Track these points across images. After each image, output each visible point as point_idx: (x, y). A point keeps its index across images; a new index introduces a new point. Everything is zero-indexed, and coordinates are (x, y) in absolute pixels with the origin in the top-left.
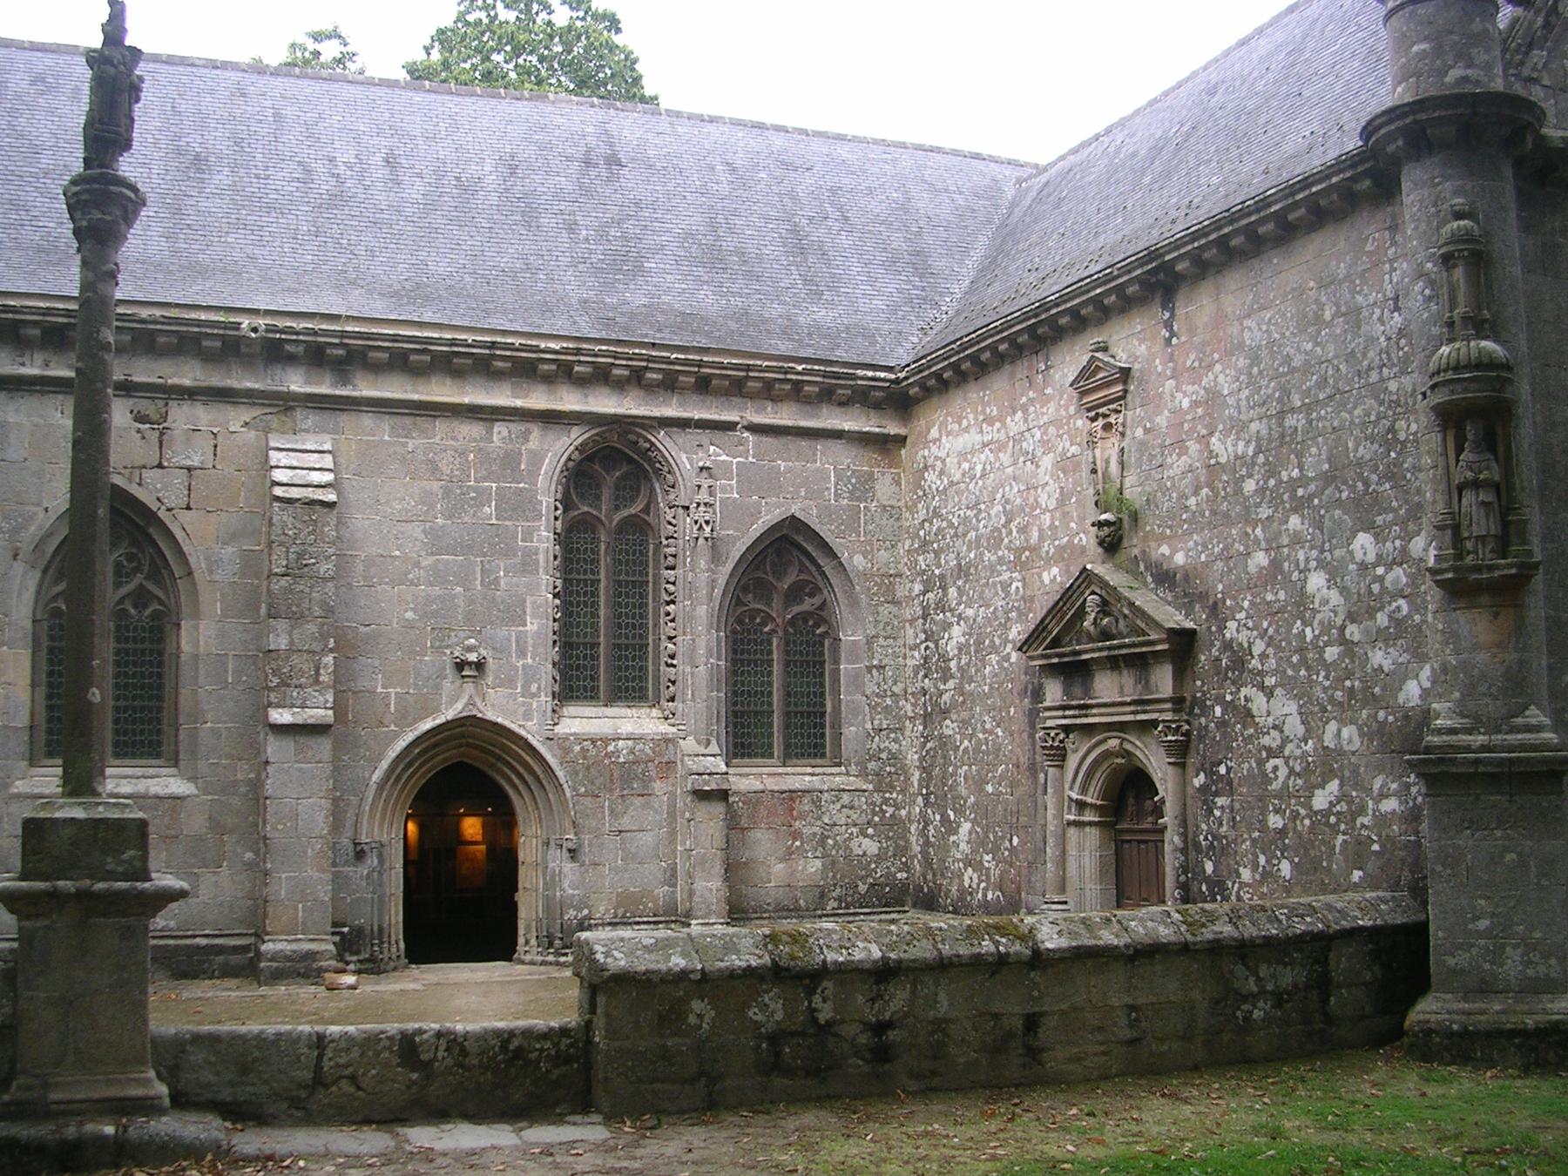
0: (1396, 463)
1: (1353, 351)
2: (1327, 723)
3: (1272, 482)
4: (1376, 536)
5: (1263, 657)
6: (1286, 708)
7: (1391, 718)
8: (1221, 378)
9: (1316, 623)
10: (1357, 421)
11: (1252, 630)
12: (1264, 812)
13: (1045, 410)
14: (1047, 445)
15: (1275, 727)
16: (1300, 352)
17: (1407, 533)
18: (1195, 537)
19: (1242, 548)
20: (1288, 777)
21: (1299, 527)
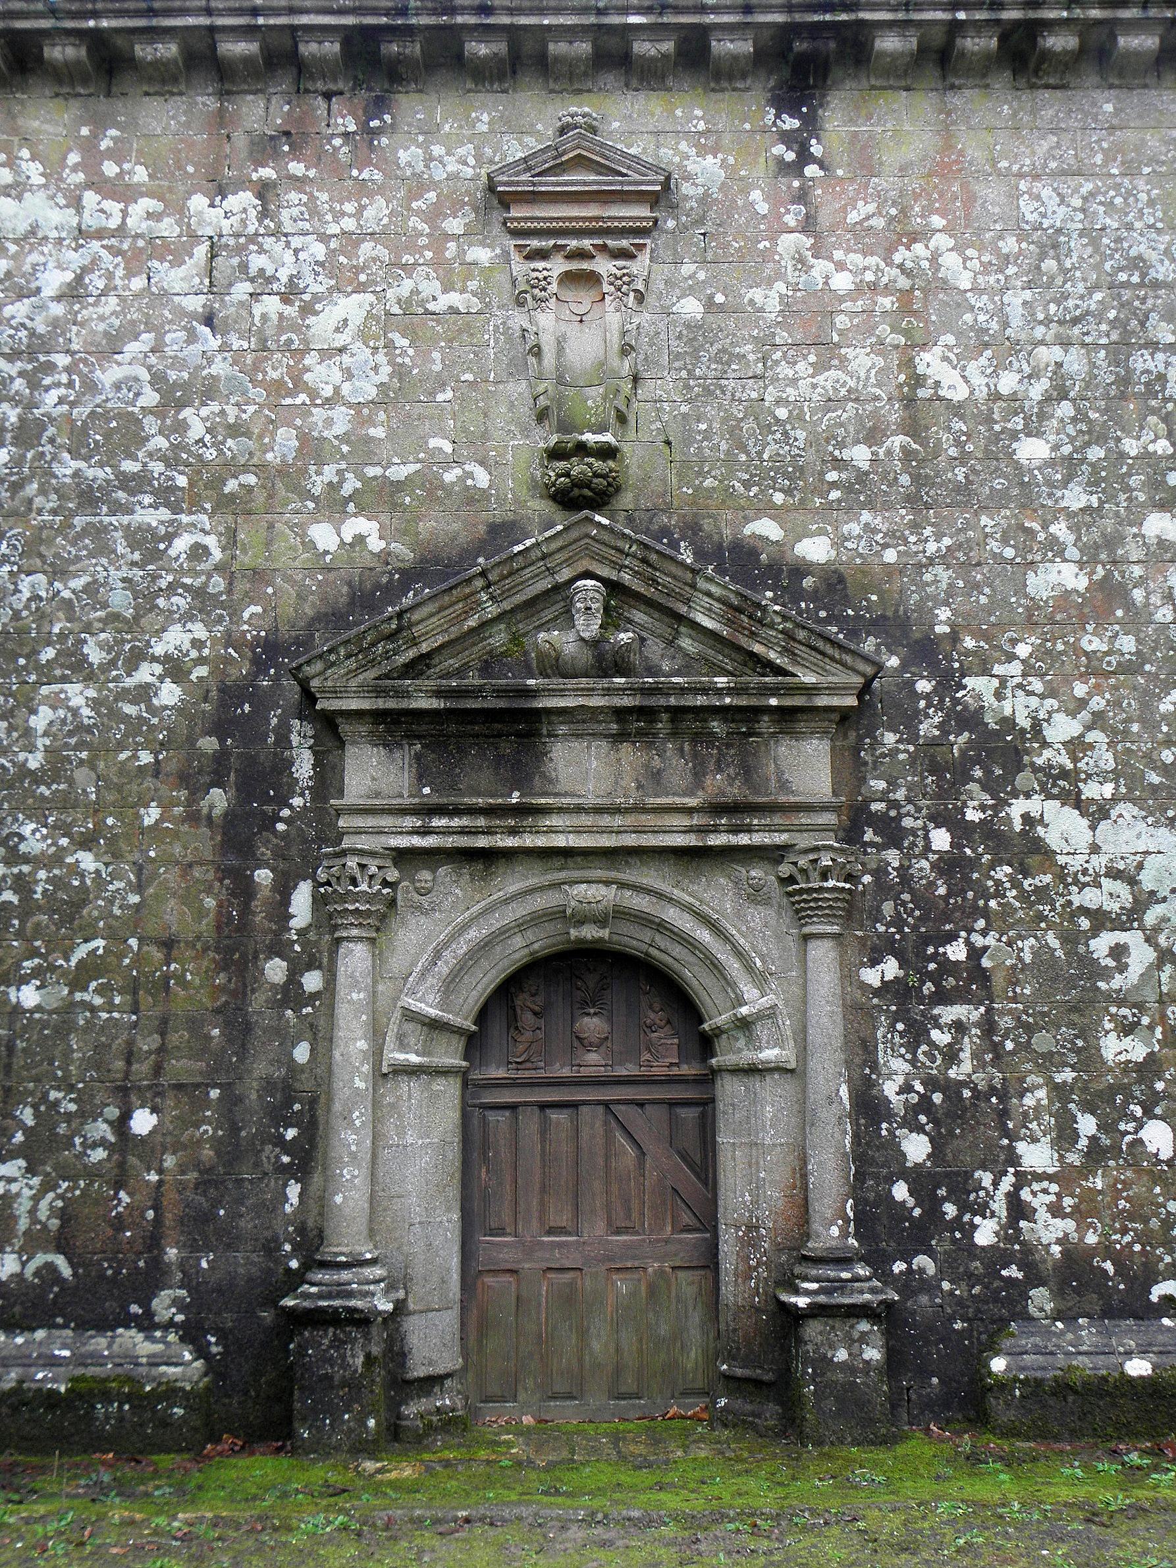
3: (1096, 453)
5: (1076, 747)
8: (950, 261)
11: (1042, 697)
12: (1090, 1033)
13: (349, 207)
15: (1114, 874)
18: (866, 516)
20: (1159, 965)
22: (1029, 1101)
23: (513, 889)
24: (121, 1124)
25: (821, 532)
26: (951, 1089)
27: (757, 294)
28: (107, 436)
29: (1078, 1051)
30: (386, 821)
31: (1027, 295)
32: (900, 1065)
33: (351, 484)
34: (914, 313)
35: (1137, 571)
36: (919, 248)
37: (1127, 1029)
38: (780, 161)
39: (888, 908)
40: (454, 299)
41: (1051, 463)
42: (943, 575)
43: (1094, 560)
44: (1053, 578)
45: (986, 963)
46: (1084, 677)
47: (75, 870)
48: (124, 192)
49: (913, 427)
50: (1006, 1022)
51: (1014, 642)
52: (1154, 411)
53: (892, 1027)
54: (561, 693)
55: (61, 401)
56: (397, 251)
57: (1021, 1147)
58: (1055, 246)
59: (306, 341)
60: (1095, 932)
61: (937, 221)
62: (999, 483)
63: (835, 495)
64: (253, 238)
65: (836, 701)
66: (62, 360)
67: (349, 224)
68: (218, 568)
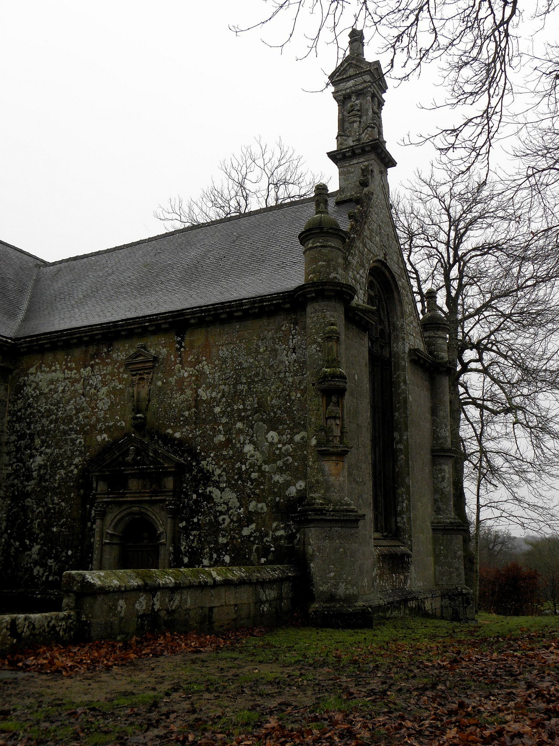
0: (289, 407)
1: (273, 365)
2: (250, 502)
3: (229, 409)
4: (278, 433)
5: (220, 476)
6: (231, 496)
7: (282, 500)
8: (206, 367)
9: (247, 464)
10: (273, 390)
12: (217, 537)
13: (105, 368)
14: (104, 384)
15: (224, 503)
16: (247, 362)
17: (294, 433)
18: (187, 427)
19: (211, 433)
20: (230, 523)
21: (241, 427)
22: (205, 551)
23: (124, 508)
24: (67, 553)
25: (179, 431)
26: (192, 548)
27: (171, 379)
28: (68, 420)
29: (214, 540)
30: (103, 496)
31: (219, 374)
32: (184, 543)
33: (104, 427)
34: (198, 380)
35: (234, 436)
36: (200, 365)
37: (224, 536)
38: (177, 347)
39: (185, 511)
40: (121, 386)
41: (220, 412)
42: (199, 439)
43: (226, 434)
44: (219, 439)
45: (200, 522)
46: (222, 460)
47: (62, 506)
48: (70, 369)
49: (196, 407)
50: (203, 535)
51: (211, 453)
52: (240, 398)
53: (183, 536)
54: (127, 470)
55: (61, 414)
56: (112, 377)
57: (203, 560)
58: (225, 362)
59: (98, 398)
60: (220, 516)
61: (204, 358)
62: (211, 418)
63: (182, 423)
64: (90, 377)
65: (171, 470)
66: (61, 405)
67: (105, 372)
68: (83, 446)
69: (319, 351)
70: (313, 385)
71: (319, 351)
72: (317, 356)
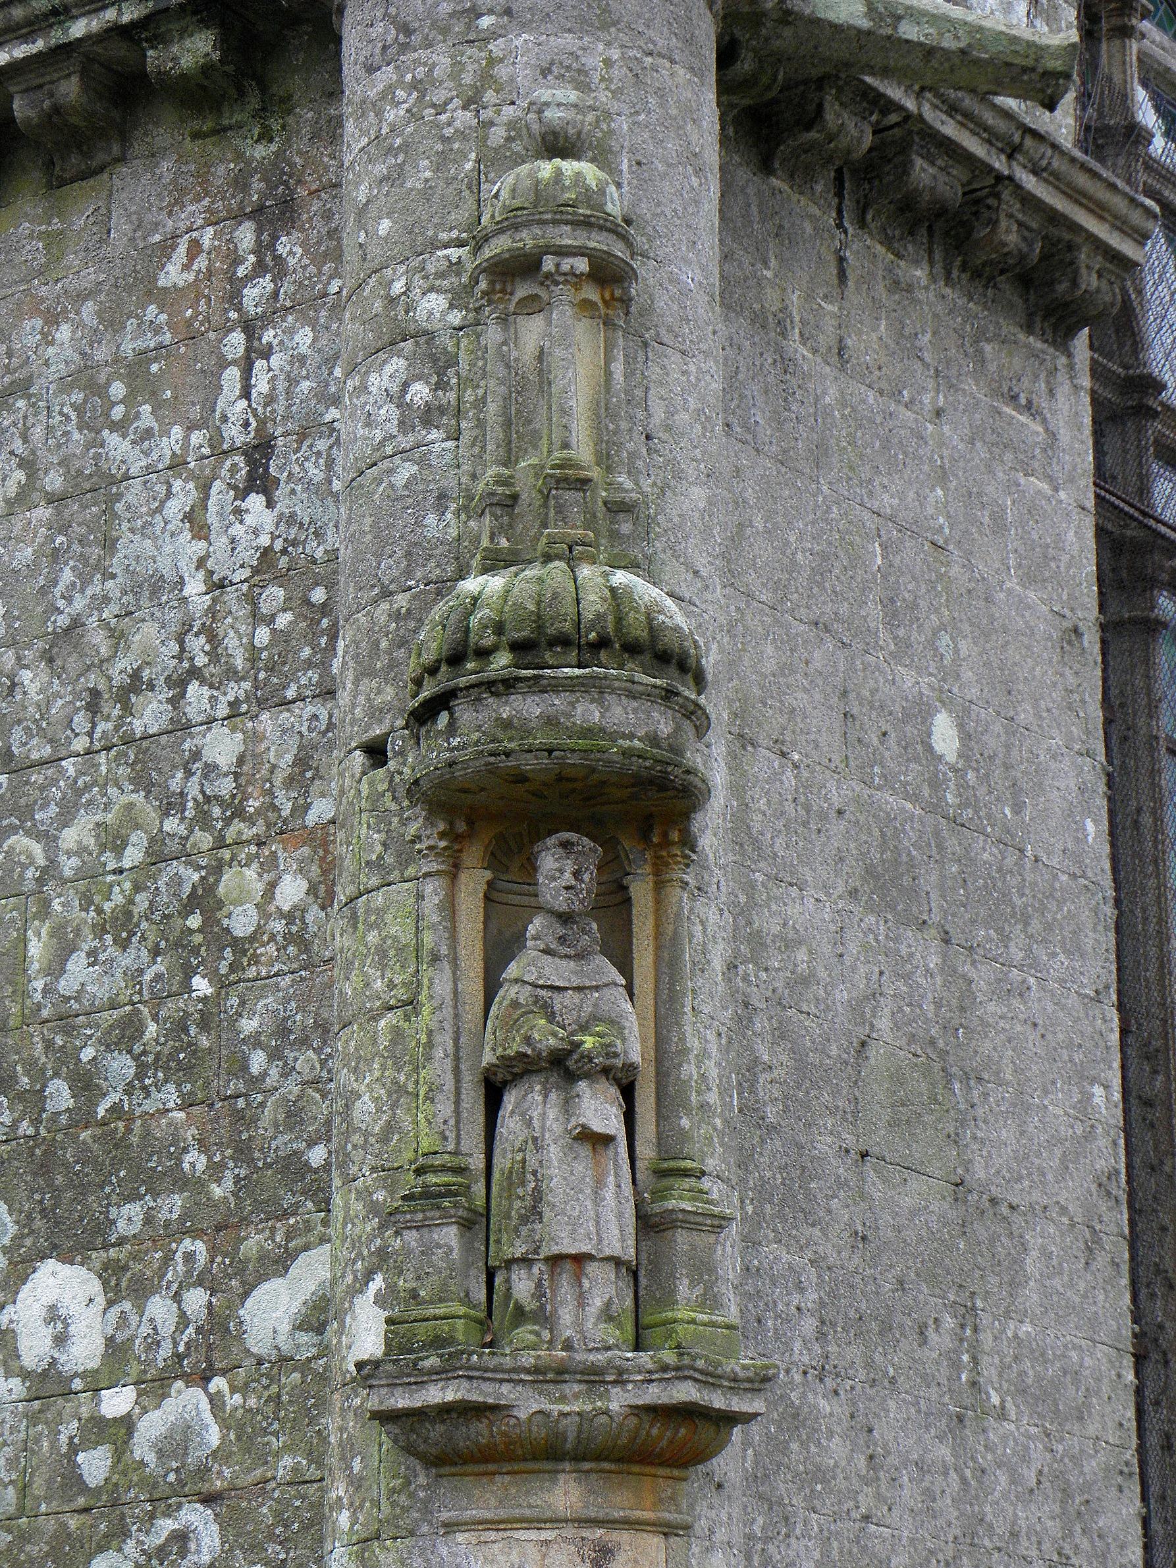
1: (76, 623)
4: (110, 1274)
10: (69, 866)
17: (240, 1268)
69: (429, 416)
70: (376, 752)
71: (429, 416)
72: (406, 471)
